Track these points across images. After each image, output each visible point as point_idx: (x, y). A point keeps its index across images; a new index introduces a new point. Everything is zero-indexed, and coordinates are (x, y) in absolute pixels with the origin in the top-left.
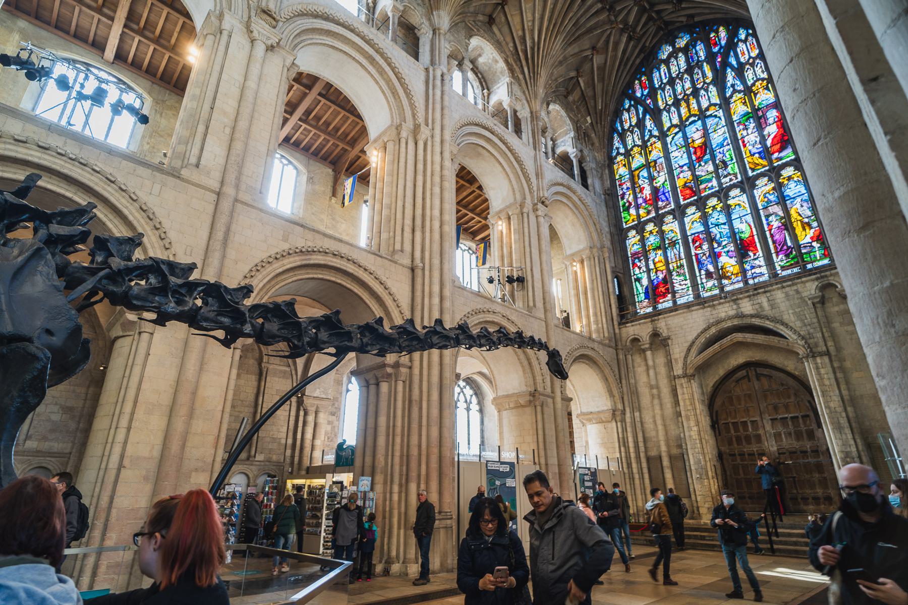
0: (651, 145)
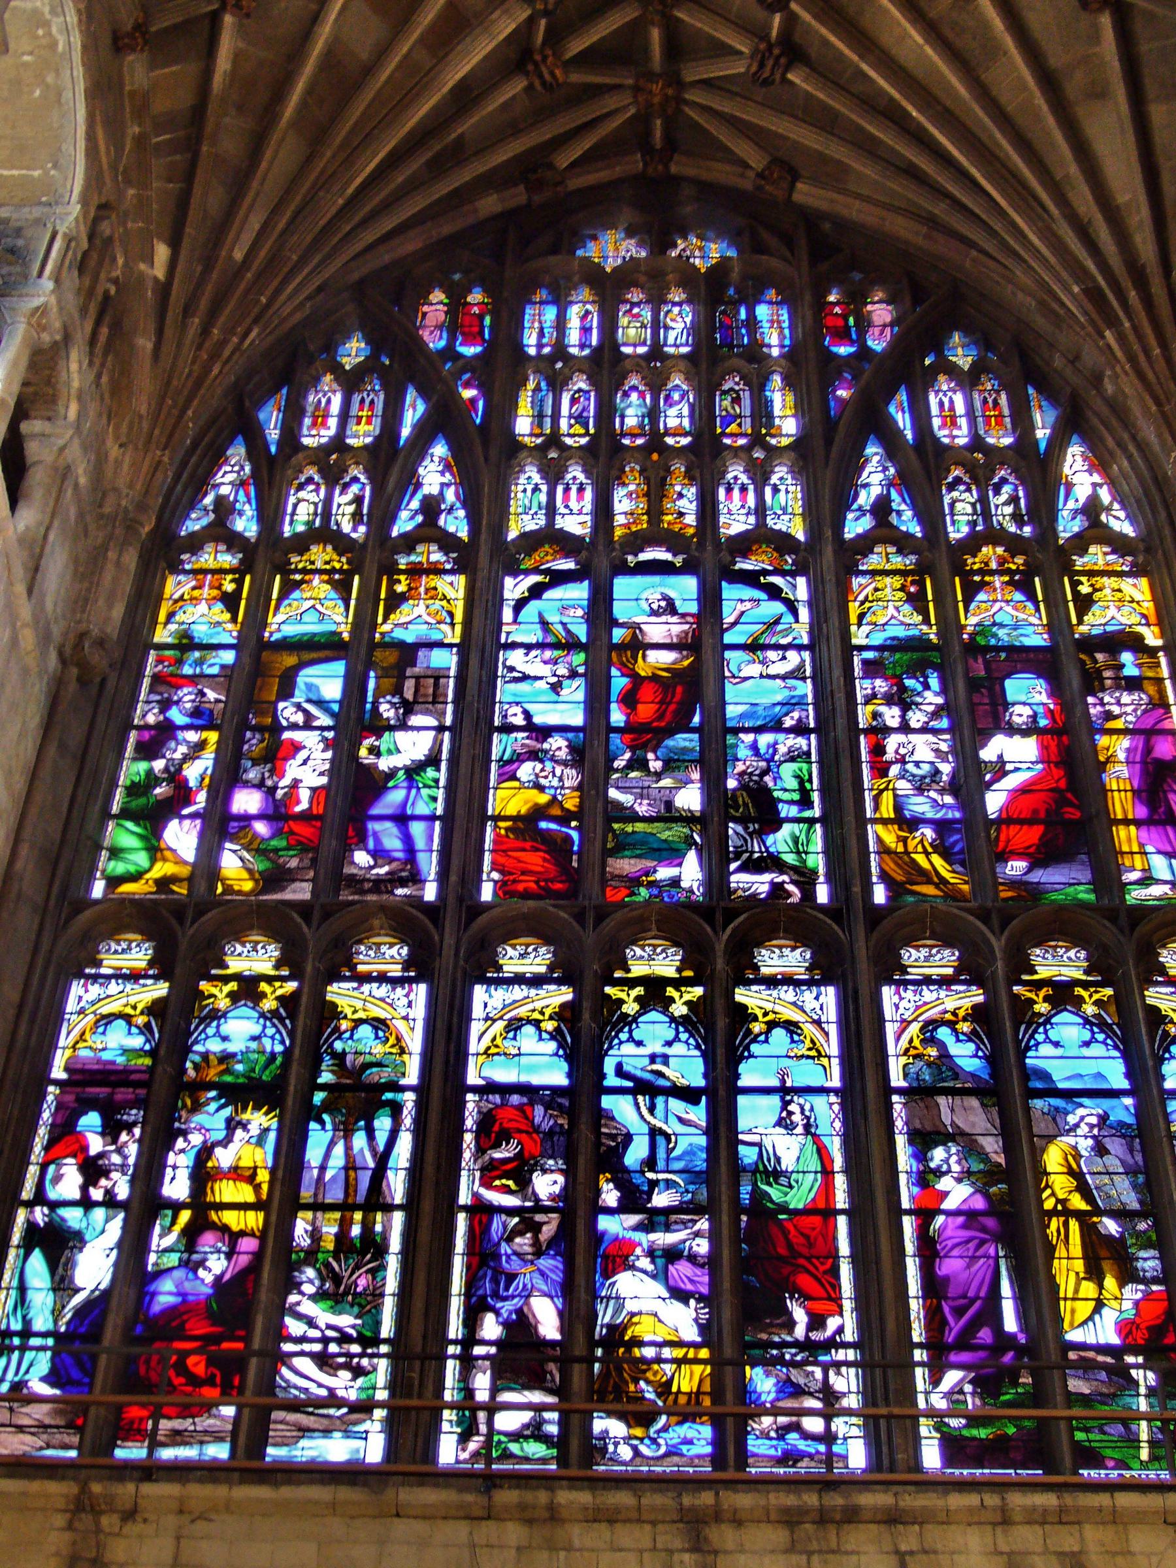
0: (416, 571)
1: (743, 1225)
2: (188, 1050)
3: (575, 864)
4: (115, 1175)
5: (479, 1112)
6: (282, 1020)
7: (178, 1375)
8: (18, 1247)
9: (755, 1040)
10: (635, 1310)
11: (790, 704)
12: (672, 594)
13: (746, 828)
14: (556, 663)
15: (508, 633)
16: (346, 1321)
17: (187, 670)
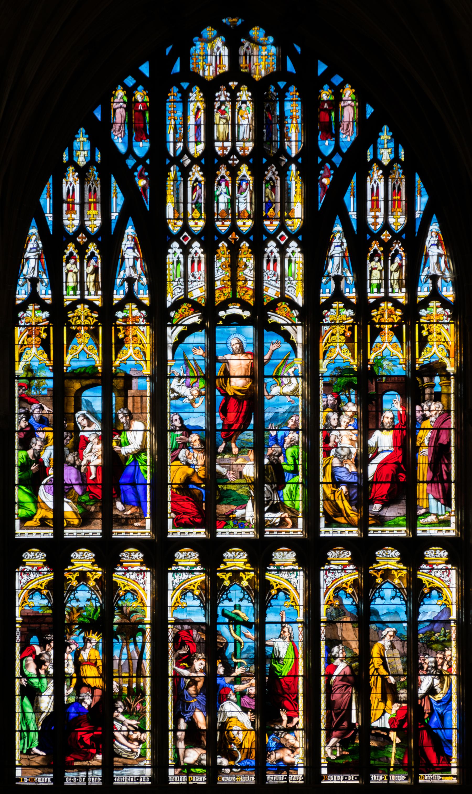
1: (267, 681)
2: (65, 606)
3: (204, 508)
4: (47, 664)
5: (173, 633)
6: (97, 591)
7: (81, 745)
8: (19, 695)
9: (272, 598)
10: (230, 716)
11: (291, 412)
12: (243, 339)
13: (272, 487)
14: (192, 387)
15: (171, 366)
16: (134, 722)
17: (33, 393)
